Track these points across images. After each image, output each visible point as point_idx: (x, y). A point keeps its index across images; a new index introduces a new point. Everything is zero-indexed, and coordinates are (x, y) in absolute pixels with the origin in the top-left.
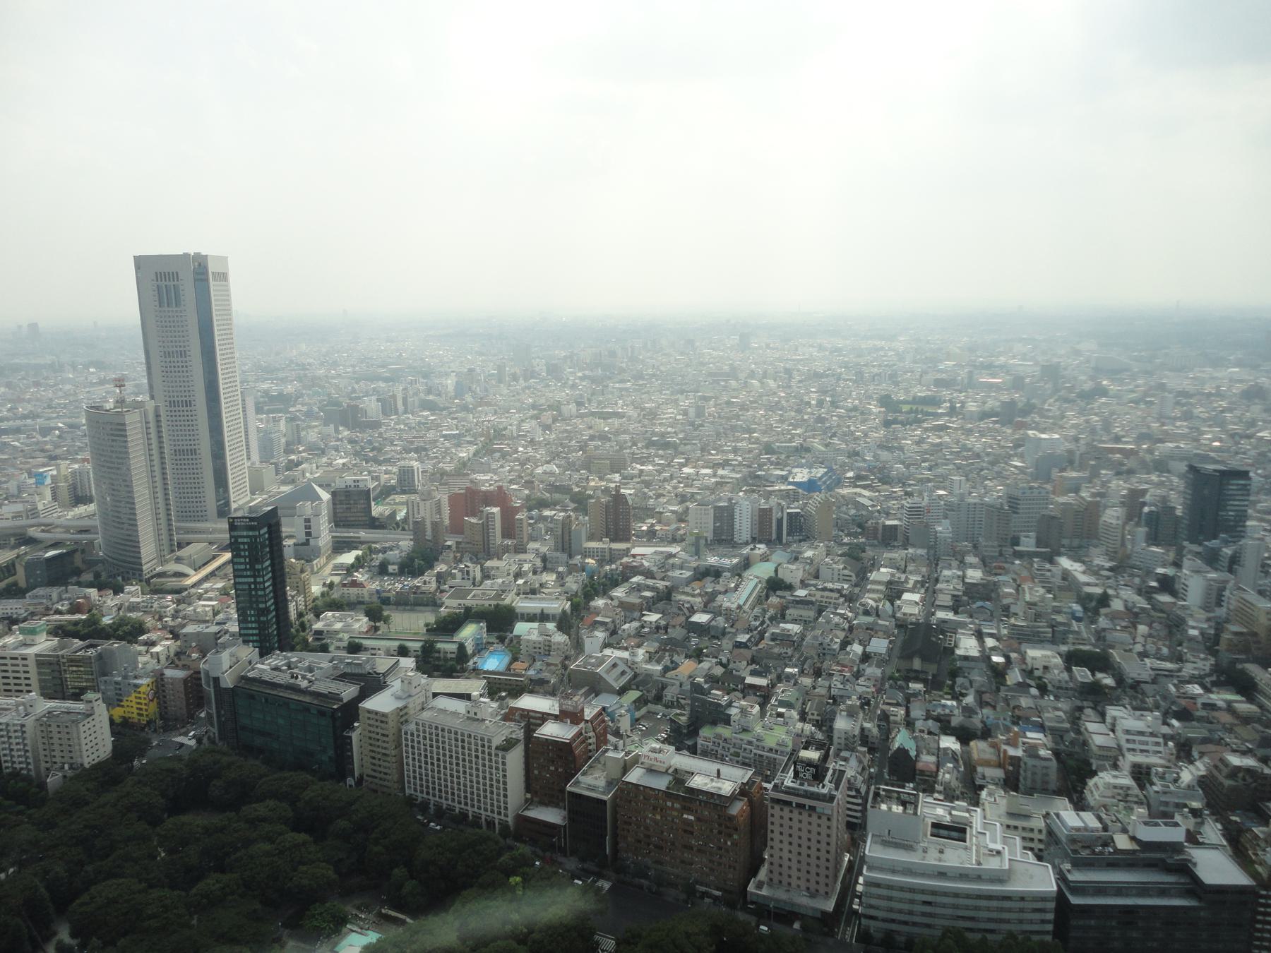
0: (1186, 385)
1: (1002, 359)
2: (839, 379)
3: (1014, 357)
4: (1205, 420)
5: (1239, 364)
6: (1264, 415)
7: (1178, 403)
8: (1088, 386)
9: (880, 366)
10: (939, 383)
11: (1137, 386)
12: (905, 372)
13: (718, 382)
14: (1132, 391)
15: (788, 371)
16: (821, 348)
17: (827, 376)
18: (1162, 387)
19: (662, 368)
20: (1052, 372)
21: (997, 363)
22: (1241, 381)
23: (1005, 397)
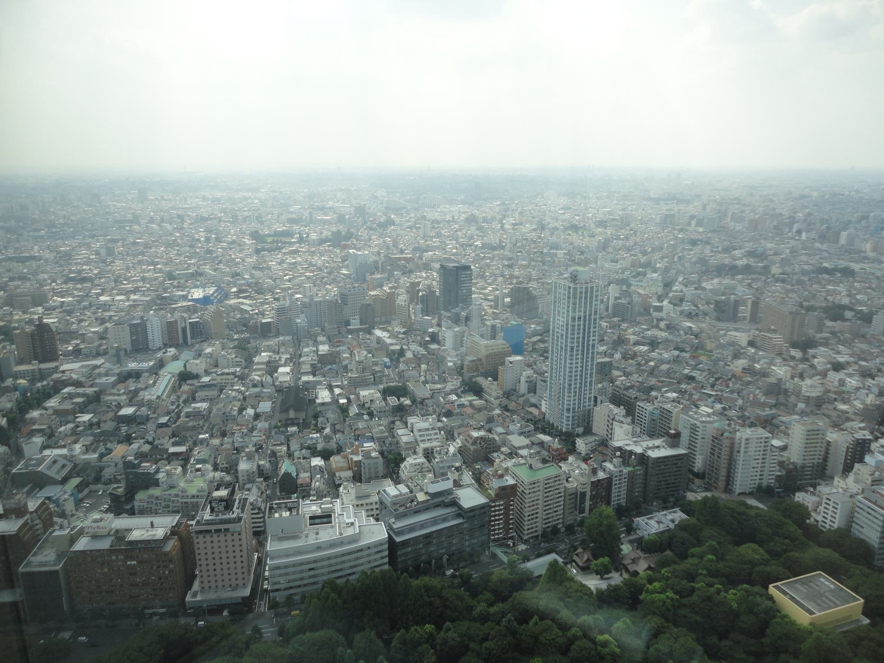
0: (437, 216)
2: (220, 221)
3: (338, 202)
4: (448, 237)
5: (463, 203)
7: (433, 227)
8: (383, 219)
9: (249, 210)
10: (291, 221)
11: (411, 218)
12: (267, 214)
13: (123, 227)
14: (408, 221)
15: (180, 217)
16: (204, 198)
17: (211, 219)
18: (424, 218)
19: (73, 218)
20: (360, 211)
21: (328, 206)
22: (465, 213)
23: (334, 229)
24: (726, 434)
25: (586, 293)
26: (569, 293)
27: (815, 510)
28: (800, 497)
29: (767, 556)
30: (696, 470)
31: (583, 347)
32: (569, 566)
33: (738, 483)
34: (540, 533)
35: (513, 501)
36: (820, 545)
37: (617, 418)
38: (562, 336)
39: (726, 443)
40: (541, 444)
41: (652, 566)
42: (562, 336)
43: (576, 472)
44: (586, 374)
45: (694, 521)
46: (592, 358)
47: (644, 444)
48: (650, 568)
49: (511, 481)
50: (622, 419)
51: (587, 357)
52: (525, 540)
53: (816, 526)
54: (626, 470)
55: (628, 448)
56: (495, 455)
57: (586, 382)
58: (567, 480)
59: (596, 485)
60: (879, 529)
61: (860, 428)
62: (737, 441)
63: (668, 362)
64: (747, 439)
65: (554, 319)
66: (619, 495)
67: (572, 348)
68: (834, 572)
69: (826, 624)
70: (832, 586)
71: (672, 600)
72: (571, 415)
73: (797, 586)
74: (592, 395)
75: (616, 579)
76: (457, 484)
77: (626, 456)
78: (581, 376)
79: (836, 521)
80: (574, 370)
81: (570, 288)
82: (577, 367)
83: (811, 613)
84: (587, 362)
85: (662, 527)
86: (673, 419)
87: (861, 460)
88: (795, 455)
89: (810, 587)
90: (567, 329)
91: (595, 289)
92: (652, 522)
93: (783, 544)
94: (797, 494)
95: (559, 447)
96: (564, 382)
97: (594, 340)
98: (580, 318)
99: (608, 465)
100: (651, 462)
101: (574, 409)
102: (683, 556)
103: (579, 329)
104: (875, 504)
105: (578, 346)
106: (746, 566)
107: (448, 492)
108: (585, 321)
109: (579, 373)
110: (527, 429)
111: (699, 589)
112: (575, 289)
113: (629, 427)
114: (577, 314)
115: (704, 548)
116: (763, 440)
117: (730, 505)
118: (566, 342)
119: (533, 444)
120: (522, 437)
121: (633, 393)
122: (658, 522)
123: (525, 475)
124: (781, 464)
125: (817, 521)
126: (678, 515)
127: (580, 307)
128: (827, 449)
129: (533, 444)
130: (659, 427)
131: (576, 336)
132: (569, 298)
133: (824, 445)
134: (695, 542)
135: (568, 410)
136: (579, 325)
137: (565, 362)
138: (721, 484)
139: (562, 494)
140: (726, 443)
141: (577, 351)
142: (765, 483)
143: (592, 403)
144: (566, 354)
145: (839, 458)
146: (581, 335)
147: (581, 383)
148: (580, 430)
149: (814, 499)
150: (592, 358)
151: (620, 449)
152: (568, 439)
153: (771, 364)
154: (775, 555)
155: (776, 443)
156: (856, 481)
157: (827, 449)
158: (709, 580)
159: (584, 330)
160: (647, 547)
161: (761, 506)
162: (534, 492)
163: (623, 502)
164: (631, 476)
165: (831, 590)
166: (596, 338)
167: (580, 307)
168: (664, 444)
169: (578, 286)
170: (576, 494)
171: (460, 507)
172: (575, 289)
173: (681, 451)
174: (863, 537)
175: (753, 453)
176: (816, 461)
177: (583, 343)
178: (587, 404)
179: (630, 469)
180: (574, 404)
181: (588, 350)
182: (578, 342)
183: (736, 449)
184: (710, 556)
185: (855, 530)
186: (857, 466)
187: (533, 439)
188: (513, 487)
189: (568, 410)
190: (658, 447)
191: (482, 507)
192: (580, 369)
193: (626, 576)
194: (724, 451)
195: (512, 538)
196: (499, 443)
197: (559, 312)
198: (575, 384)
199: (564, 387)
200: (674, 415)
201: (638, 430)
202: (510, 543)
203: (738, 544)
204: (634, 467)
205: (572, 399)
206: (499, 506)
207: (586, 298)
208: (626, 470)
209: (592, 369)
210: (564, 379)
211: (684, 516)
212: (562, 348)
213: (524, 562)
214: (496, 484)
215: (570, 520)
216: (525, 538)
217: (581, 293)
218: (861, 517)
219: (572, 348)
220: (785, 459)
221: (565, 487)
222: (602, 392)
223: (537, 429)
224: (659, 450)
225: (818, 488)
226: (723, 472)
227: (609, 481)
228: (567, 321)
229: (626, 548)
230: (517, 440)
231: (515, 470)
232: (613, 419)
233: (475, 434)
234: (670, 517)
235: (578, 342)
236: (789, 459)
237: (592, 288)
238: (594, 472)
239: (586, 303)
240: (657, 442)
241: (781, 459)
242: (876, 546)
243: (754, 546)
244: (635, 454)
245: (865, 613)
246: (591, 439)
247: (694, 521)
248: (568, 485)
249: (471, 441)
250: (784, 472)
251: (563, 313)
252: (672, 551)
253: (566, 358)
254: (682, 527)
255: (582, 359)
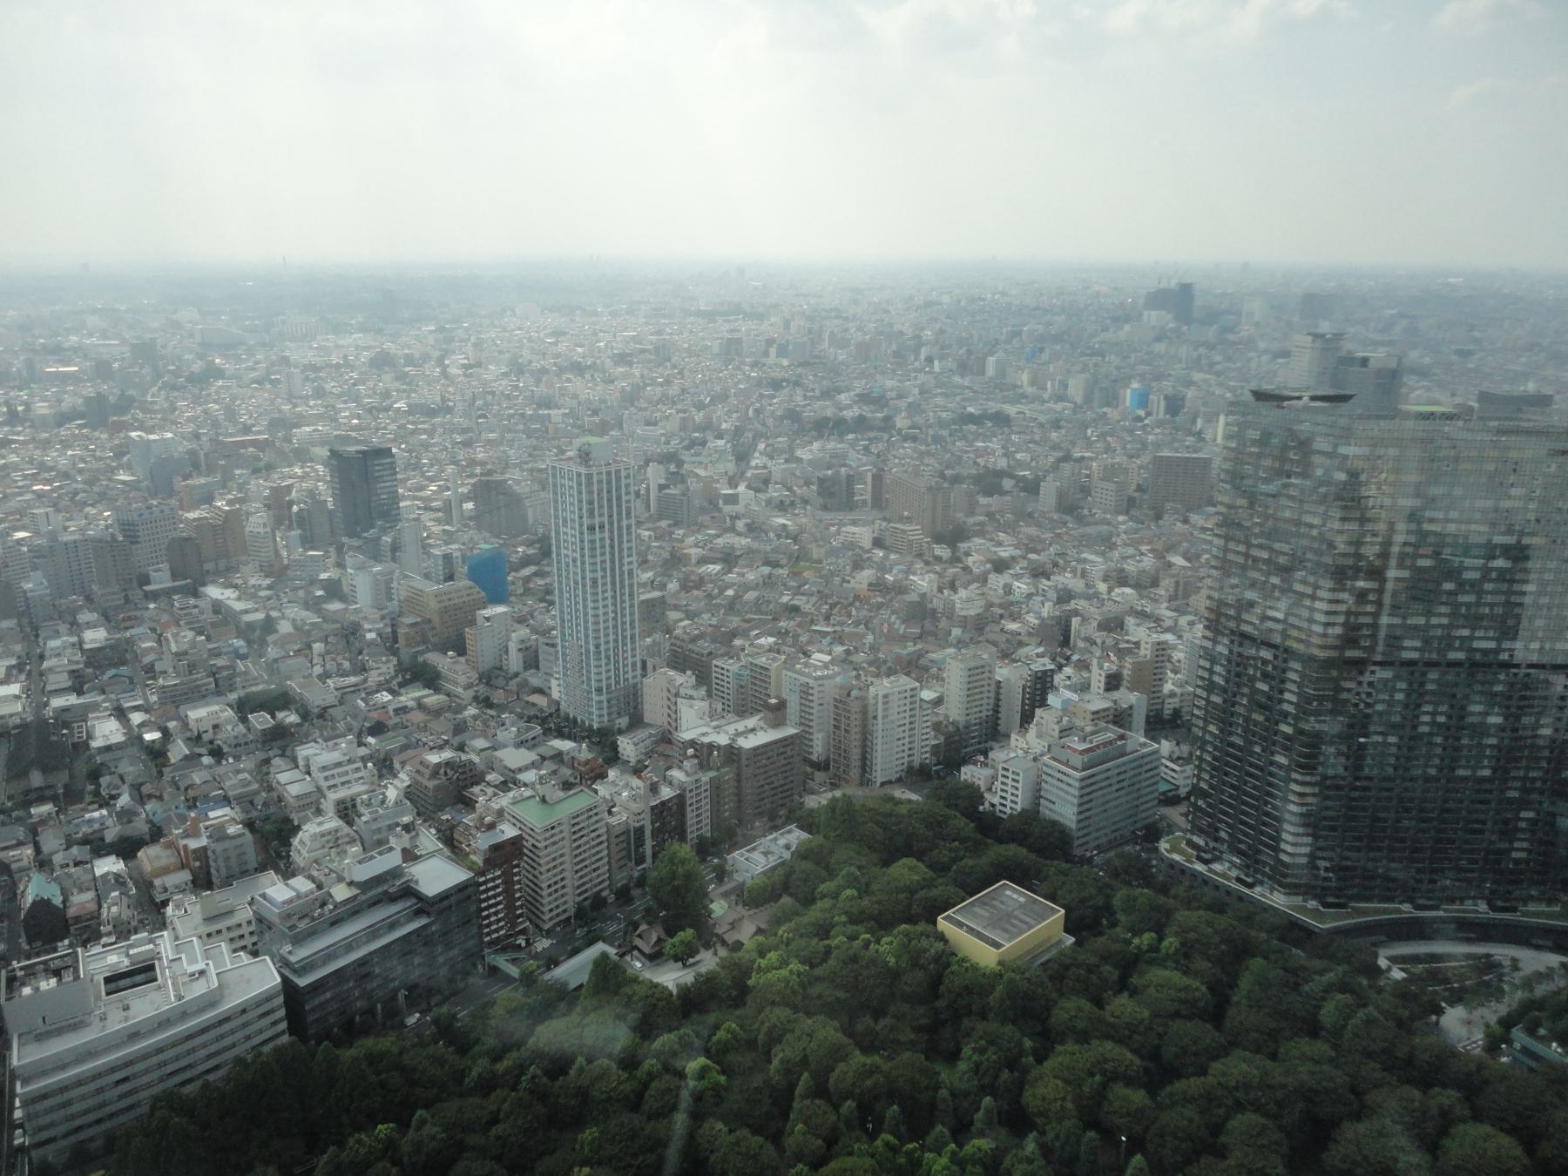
0: (310, 357)
1: (74, 338)
3: (91, 335)
4: (339, 396)
5: (363, 329)
6: (397, 384)
7: (307, 379)
8: (198, 367)
11: (257, 363)
14: (253, 369)
18: (285, 361)
20: (145, 351)
21: (67, 345)
22: (368, 348)
23: (90, 391)
24: (854, 693)
25: (609, 483)
26: (579, 484)
27: (990, 789)
28: (968, 773)
29: (930, 874)
30: (814, 757)
31: (613, 577)
32: (628, 958)
33: (879, 767)
34: (572, 912)
35: (518, 866)
36: (1000, 841)
37: (683, 691)
38: (574, 561)
39: (855, 707)
40: (558, 757)
41: (763, 926)
42: (574, 561)
43: (623, 796)
44: (623, 623)
45: (818, 840)
46: (631, 595)
47: (731, 729)
48: (760, 931)
49: (508, 831)
50: (690, 692)
51: (622, 595)
52: (548, 931)
53: (993, 814)
54: (706, 777)
55: (706, 740)
56: (476, 789)
57: (624, 637)
58: (610, 812)
59: (660, 811)
60: (1076, 801)
61: (1038, 655)
62: (872, 701)
63: (756, 587)
64: (885, 696)
65: (557, 533)
66: (699, 822)
67: (595, 581)
68: (1022, 877)
69: (1019, 957)
70: (1022, 899)
71: (799, 974)
72: (604, 698)
73: (976, 909)
74: (638, 659)
75: (708, 961)
76: (410, 856)
77: (703, 753)
78: (615, 627)
79: (1019, 800)
80: (601, 619)
81: (579, 475)
82: (606, 614)
83: (997, 945)
84: (623, 602)
85: (773, 861)
86: (773, 680)
87: (1043, 703)
88: (955, 711)
89: (994, 907)
90: (582, 549)
91: (623, 474)
92: (757, 856)
93: (950, 850)
94: (963, 769)
95: (590, 756)
96: (587, 643)
97: (630, 563)
98: (602, 527)
99: (677, 774)
100: (744, 757)
101: (609, 686)
102: (809, 901)
103: (603, 547)
104: (1067, 764)
105: (604, 577)
106: (902, 896)
107: (394, 873)
108: (612, 532)
109: (610, 623)
110: (530, 735)
111: (837, 947)
112: (589, 477)
113: (703, 704)
114: (597, 521)
115: (839, 880)
116: (908, 694)
117: (870, 804)
118: (583, 571)
119: (543, 758)
120: (523, 751)
121: (704, 646)
122: (766, 854)
123: (534, 817)
124: (937, 727)
125: (993, 805)
126: (795, 836)
127: (601, 507)
128: (998, 694)
129: (543, 758)
130: (752, 698)
131: (599, 559)
132: (580, 493)
133: (993, 688)
134: (824, 873)
135: (599, 690)
136: (602, 540)
137: (585, 607)
138: (855, 773)
139: (604, 838)
140: (855, 707)
141: (604, 584)
142: (916, 764)
143: (639, 672)
144: (584, 592)
145: (1013, 704)
146: (608, 557)
147: (616, 641)
148: (623, 722)
149: (987, 772)
150: (631, 595)
151: (692, 743)
152: (605, 742)
153: (909, 571)
154: (940, 868)
155: (927, 695)
156: (1040, 736)
157: (998, 694)
158: (851, 928)
159: (612, 547)
160: (753, 898)
161: (914, 797)
162: (554, 843)
163: (706, 831)
164: (716, 787)
165: (1022, 906)
166: (634, 558)
167: (601, 507)
168: (762, 724)
169: (594, 470)
170: (627, 832)
171: (419, 896)
172: (589, 477)
173: (790, 731)
174: (1055, 817)
175: (896, 716)
176: (984, 714)
177: (613, 570)
178: (630, 675)
179: (712, 774)
180: (608, 678)
181: (622, 582)
182: (604, 570)
183: (871, 715)
184: (848, 892)
185: (1046, 811)
186: (1038, 712)
187: (542, 750)
188: (516, 842)
189: (599, 690)
190: (753, 730)
191: (462, 888)
192: (611, 615)
193: (723, 952)
194: (854, 717)
195: (523, 932)
196: (481, 767)
197: (565, 521)
198: (607, 643)
199: (588, 651)
200: (773, 674)
201: (719, 707)
202: (521, 941)
203: (887, 863)
204: (718, 769)
205: (603, 669)
206: (493, 880)
207: (609, 492)
208: (706, 777)
209: (632, 614)
210: (587, 636)
211: (805, 835)
212: (576, 583)
213: (549, 969)
214: (483, 842)
215: (621, 879)
216: (546, 927)
217: (600, 482)
218: (1050, 789)
219: (595, 581)
220: (941, 718)
221: (607, 824)
222: (654, 650)
223: (547, 732)
224: (755, 735)
225: (991, 755)
226: (855, 754)
227: (680, 799)
228: (582, 533)
229: (718, 908)
230: (514, 757)
231: (519, 811)
232: (677, 695)
233: (434, 758)
234: (782, 842)
235: (604, 570)
236: (947, 716)
237: (618, 471)
238: (654, 789)
239: (610, 500)
240: (751, 722)
241: (935, 719)
242: (1073, 826)
243: (911, 861)
244: (719, 748)
245: (1067, 930)
246: (641, 734)
247: (818, 840)
248: (613, 821)
249: (427, 772)
250: (942, 739)
251: (573, 520)
252: (791, 895)
253: (585, 600)
254: (803, 854)
255: (614, 597)
